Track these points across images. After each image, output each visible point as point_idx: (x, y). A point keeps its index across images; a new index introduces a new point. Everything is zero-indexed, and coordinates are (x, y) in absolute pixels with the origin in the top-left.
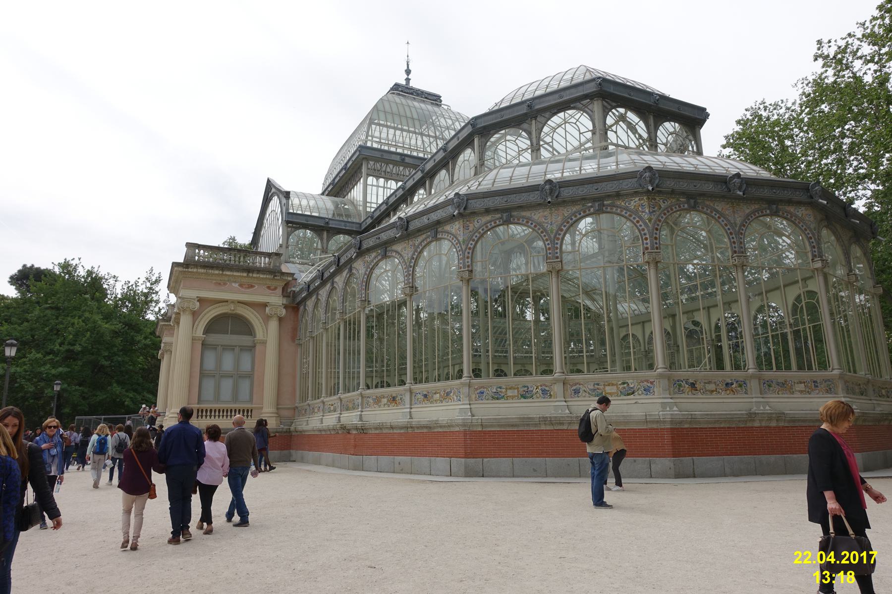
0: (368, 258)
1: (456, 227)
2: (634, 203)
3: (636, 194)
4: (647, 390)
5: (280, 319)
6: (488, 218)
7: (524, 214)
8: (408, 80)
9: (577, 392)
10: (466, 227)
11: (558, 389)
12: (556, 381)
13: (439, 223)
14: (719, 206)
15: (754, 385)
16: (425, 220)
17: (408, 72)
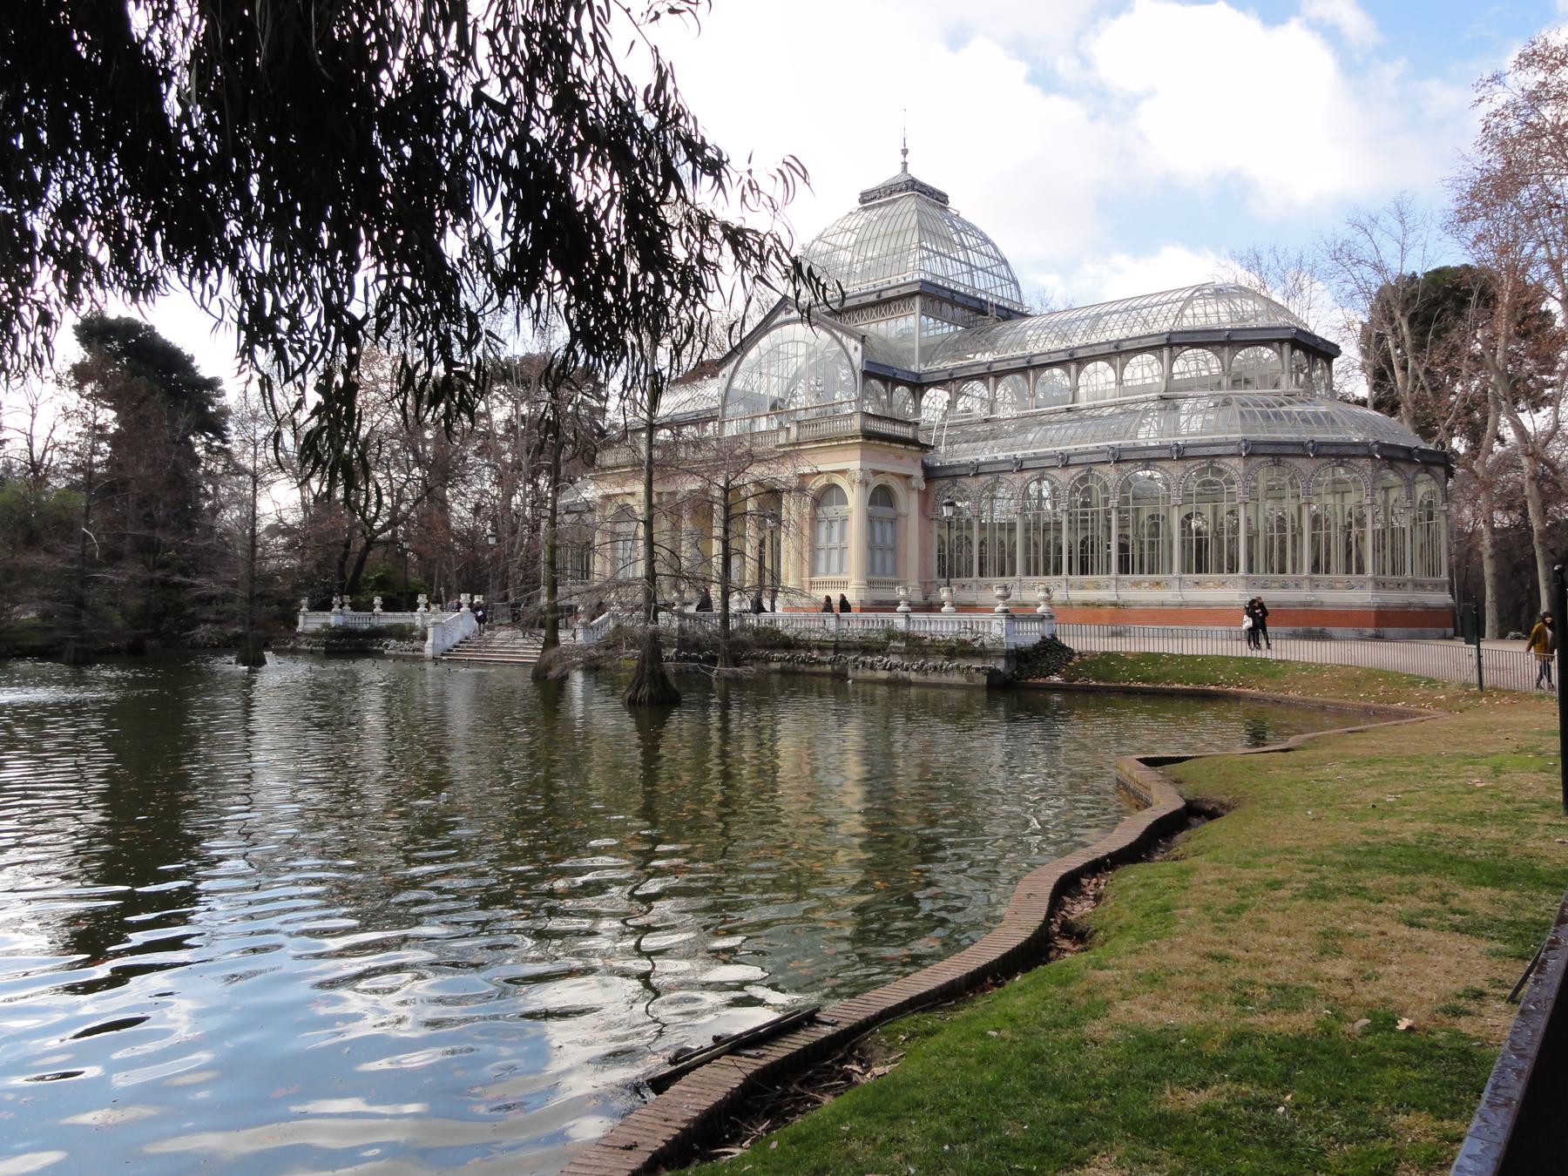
0: (1122, 466)
1: (1235, 461)
2: (1362, 462)
3: (1364, 456)
4: (1362, 587)
5: (919, 491)
6: (1263, 459)
7: (1288, 460)
8: (905, 164)
9: (1317, 586)
10: (1245, 464)
11: (1306, 583)
12: (1306, 578)
13: (1218, 456)
14: (1403, 466)
15: (1410, 585)
16: (1204, 451)
17: (905, 152)
